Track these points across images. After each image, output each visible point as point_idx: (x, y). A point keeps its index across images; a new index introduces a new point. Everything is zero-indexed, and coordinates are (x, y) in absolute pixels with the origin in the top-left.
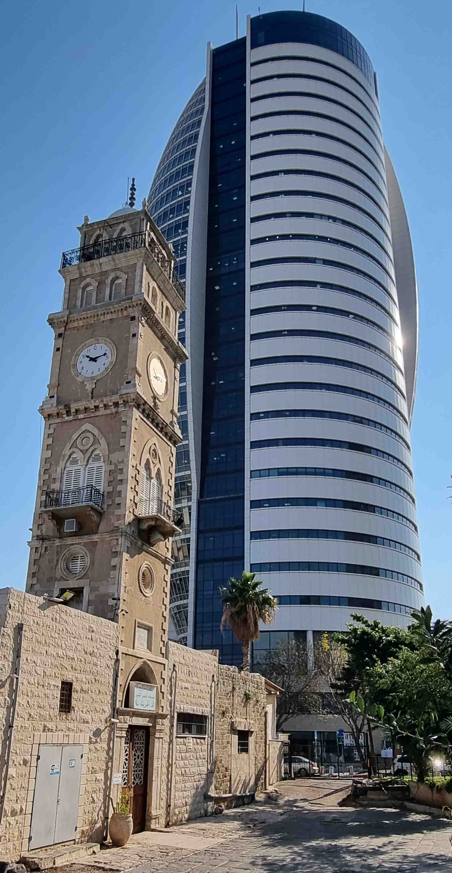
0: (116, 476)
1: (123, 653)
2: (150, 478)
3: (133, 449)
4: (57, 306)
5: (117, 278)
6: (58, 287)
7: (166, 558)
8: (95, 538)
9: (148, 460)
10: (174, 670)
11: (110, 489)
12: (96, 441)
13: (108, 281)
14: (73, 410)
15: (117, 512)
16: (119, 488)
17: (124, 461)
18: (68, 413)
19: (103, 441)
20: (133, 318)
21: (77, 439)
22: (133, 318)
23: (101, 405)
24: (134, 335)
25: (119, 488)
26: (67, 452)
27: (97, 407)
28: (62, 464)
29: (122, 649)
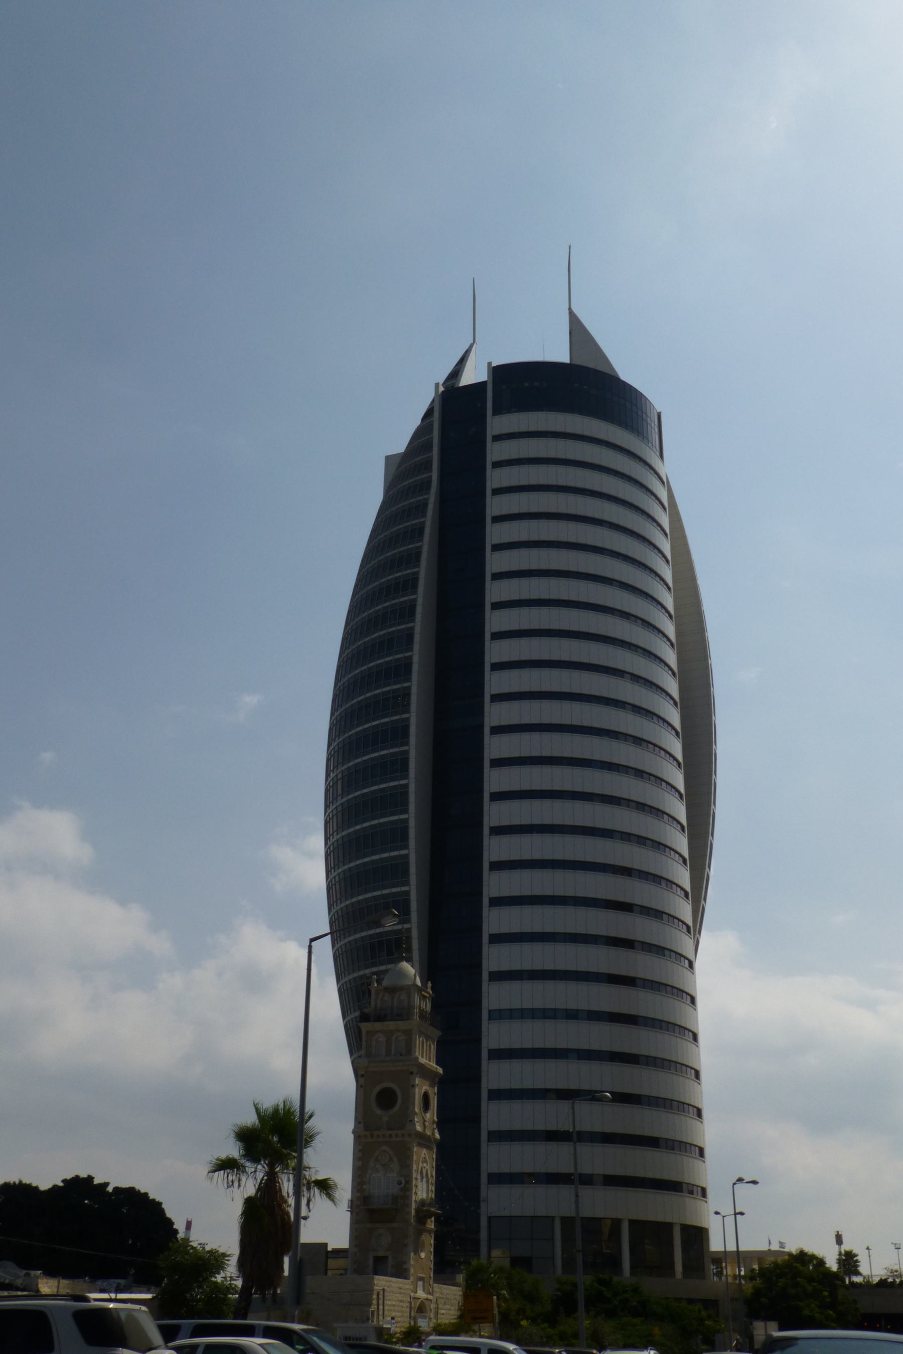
0: (406, 1187)
2: (422, 1178)
3: (415, 1167)
18: (372, 1136)
19: (395, 1159)
20: (412, 1073)
22: (412, 1073)
24: (413, 1086)
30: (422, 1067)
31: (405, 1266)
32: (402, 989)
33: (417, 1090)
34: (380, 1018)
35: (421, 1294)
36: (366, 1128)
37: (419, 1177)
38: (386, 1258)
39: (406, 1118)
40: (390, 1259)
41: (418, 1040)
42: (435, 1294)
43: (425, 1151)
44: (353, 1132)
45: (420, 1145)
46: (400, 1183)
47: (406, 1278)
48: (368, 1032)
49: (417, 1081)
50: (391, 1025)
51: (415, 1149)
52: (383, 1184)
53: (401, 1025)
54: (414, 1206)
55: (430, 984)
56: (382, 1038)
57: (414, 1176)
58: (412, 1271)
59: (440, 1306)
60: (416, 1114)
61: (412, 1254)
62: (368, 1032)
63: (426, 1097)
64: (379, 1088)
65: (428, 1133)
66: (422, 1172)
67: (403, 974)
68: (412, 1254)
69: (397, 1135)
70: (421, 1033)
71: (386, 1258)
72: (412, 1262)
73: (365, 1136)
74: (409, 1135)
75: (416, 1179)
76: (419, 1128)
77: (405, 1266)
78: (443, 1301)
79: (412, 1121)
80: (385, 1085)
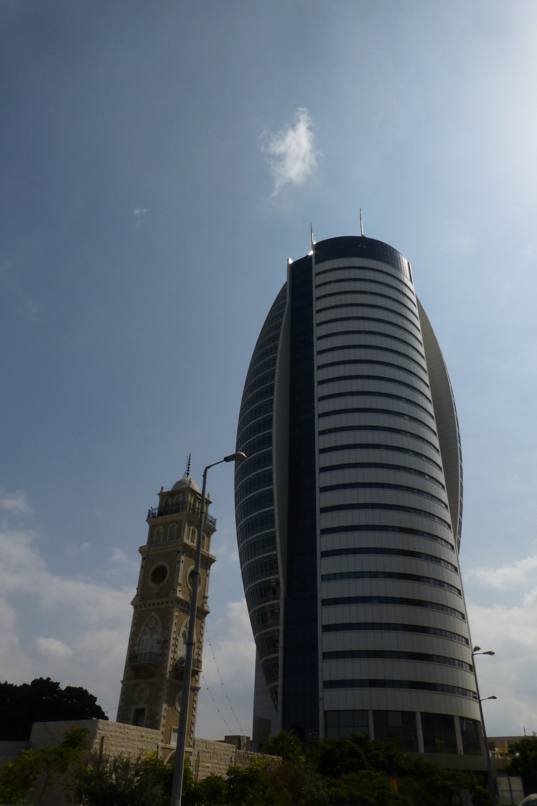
0: (164, 644)
1: (162, 748)
3: (174, 628)
4: (143, 541)
5: (173, 526)
6: (146, 528)
13: (169, 529)
14: (147, 605)
17: (169, 636)
18: (145, 605)
20: (179, 552)
22: (179, 552)
24: (179, 562)
26: (142, 629)
27: (158, 603)
28: (140, 635)
29: (161, 744)
30: (186, 546)
32: (180, 492)
33: (182, 566)
39: (172, 587)
42: (197, 748)
45: (181, 610)
47: (157, 728)
49: (183, 558)
51: (176, 614)
53: (175, 516)
54: (170, 662)
56: (162, 529)
57: (173, 636)
58: (163, 722)
60: (180, 585)
61: (165, 706)
64: (154, 567)
68: (165, 706)
69: (163, 603)
70: (190, 524)
72: (164, 713)
73: (141, 606)
74: (172, 602)
76: (180, 595)
77: (157, 718)
78: (208, 755)
79: (175, 590)
80: (160, 564)
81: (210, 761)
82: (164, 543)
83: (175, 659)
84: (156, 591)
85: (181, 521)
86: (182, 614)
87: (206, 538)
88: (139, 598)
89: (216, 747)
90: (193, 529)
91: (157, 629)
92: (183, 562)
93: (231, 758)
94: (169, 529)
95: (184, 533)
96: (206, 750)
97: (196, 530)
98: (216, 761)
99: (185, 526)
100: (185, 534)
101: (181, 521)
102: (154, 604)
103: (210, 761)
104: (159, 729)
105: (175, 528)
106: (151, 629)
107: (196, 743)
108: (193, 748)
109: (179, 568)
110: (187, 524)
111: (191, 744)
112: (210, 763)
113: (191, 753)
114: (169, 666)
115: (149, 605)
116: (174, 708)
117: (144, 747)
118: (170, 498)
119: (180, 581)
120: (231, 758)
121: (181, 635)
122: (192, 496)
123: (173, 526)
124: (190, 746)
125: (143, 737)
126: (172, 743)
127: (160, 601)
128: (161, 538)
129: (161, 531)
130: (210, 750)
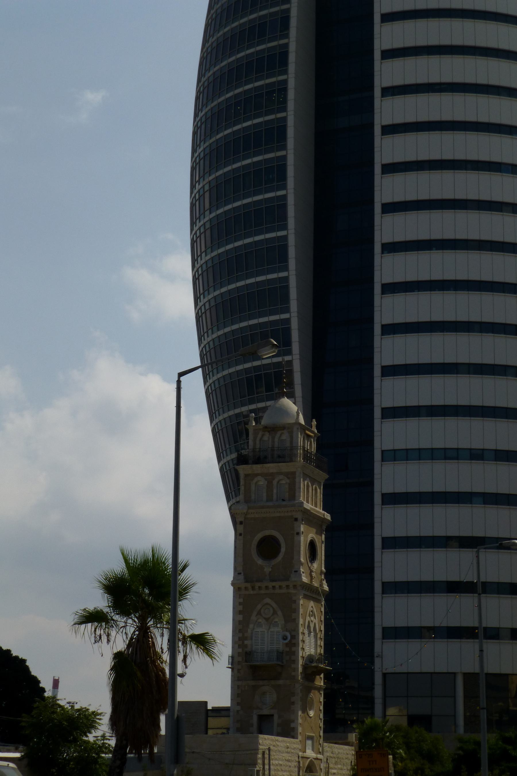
2: (310, 632)
3: (301, 621)
5: (281, 480)
7: (321, 686)
8: (281, 682)
9: (309, 621)
10: (327, 762)
11: (288, 649)
12: (275, 613)
14: (257, 587)
15: (293, 666)
16: (293, 649)
19: (279, 613)
20: (296, 520)
21: (261, 609)
22: (296, 520)
23: (277, 587)
24: (298, 534)
25: (293, 649)
26: (254, 618)
28: (251, 626)
30: (306, 512)
31: (292, 725)
32: (283, 428)
33: (302, 538)
34: (259, 460)
35: (310, 753)
36: (247, 580)
37: (306, 632)
38: (273, 715)
39: (290, 568)
40: (276, 717)
41: (303, 484)
43: (312, 603)
44: (233, 584)
45: (306, 597)
46: (285, 638)
48: (246, 476)
49: (302, 528)
50: (271, 467)
51: (301, 602)
52: (267, 638)
53: (284, 467)
54: (301, 662)
55: (314, 423)
56: (262, 482)
57: (301, 630)
58: (300, 730)
59: (331, 766)
60: (302, 564)
61: (300, 713)
62: (246, 476)
63: (312, 546)
65: (316, 584)
66: (309, 626)
67: (284, 412)
68: (300, 713)
70: (306, 476)
71: (273, 715)
72: (300, 721)
73: (246, 589)
74: (295, 587)
75: (303, 634)
76: (305, 579)
77: (292, 725)
78: (333, 760)
80: (267, 533)
81: (336, 767)
82: (270, 504)
83: (303, 657)
84: (267, 570)
85: (294, 473)
86: (306, 601)
87: (318, 490)
88: (242, 577)
89: (339, 751)
90: (308, 483)
91: (276, 620)
92: (302, 533)
93: (351, 762)
94: (275, 482)
95: (300, 492)
96: (332, 755)
97: (310, 483)
98: (339, 766)
99: (300, 483)
100: (302, 494)
101: (294, 473)
102: (267, 588)
103: (336, 767)
104: (297, 738)
105: (283, 482)
106: (267, 619)
107: (325, 749)
108: (323, 755)
109: (300, 542)
110: (302, 479)
111: (321, 750)
112: (336, 769)
113: (321, 760)
114: (300, 666)
115: (260, 588)
116: (306, 713)
117: (290, 758)
118: (267, 434)
119: (302, 560)
120: (351, 762)
121: (306, 628)
122: (301, 435)
123: (281, 480)
124: (320, 752)
125: (288, 748)
126: (307, 751)
127: (277, 584)
128: (265, 495)
129: (261, 483)
130: (335, 755)
